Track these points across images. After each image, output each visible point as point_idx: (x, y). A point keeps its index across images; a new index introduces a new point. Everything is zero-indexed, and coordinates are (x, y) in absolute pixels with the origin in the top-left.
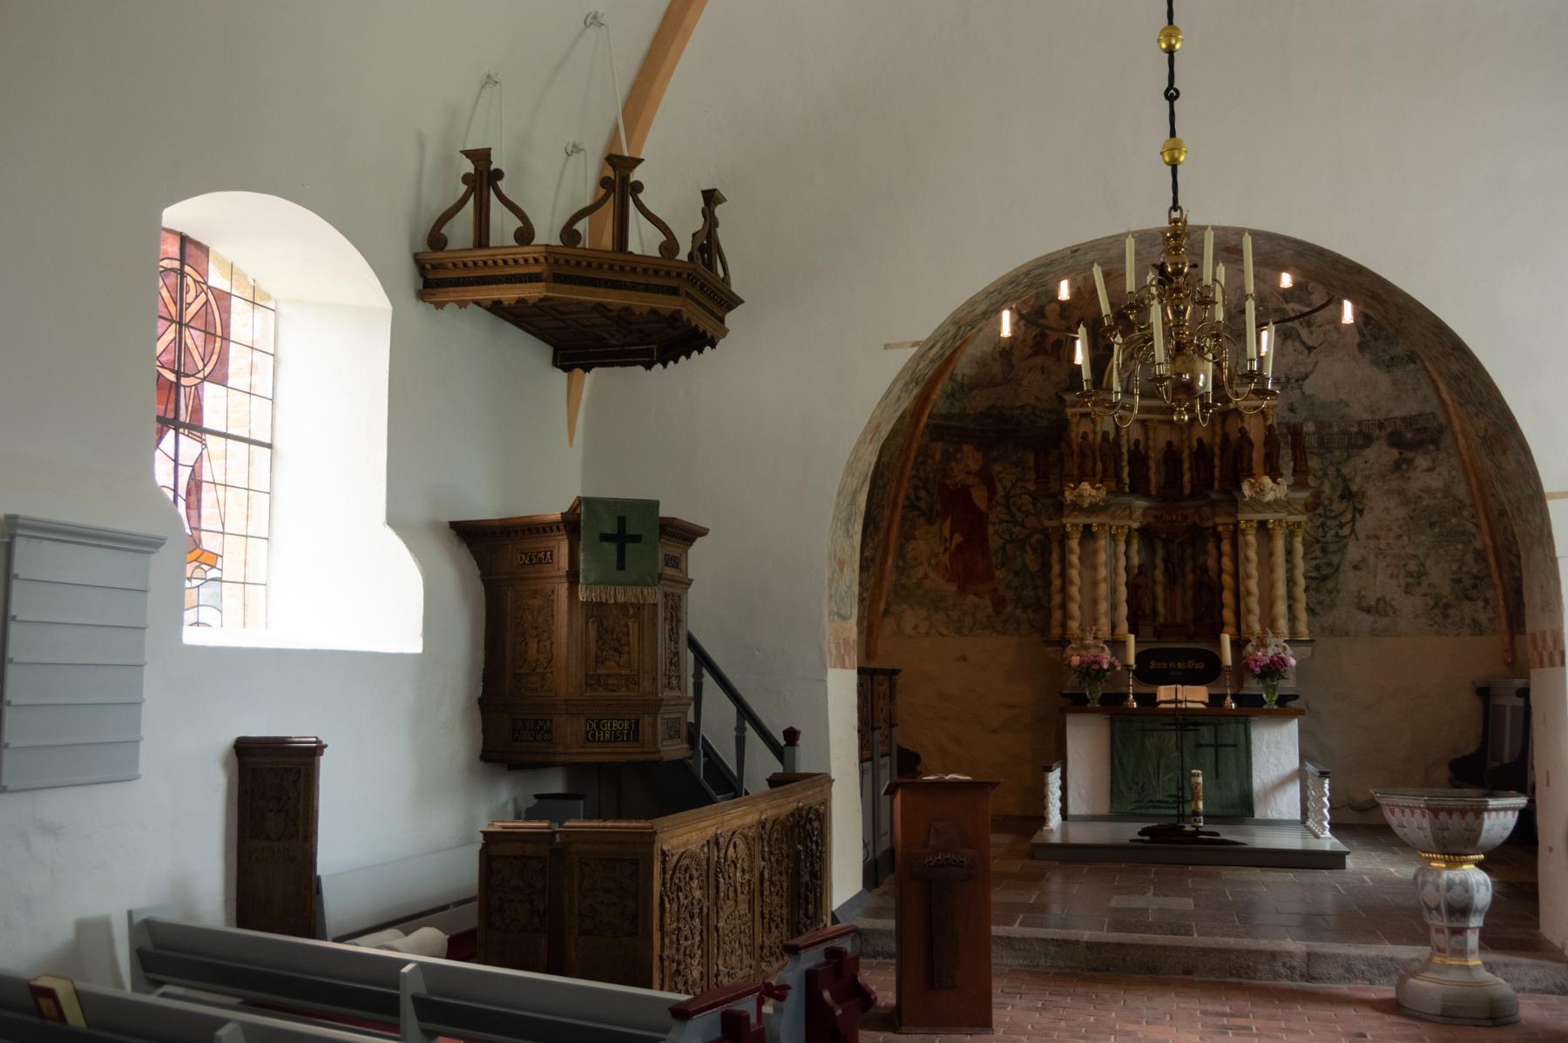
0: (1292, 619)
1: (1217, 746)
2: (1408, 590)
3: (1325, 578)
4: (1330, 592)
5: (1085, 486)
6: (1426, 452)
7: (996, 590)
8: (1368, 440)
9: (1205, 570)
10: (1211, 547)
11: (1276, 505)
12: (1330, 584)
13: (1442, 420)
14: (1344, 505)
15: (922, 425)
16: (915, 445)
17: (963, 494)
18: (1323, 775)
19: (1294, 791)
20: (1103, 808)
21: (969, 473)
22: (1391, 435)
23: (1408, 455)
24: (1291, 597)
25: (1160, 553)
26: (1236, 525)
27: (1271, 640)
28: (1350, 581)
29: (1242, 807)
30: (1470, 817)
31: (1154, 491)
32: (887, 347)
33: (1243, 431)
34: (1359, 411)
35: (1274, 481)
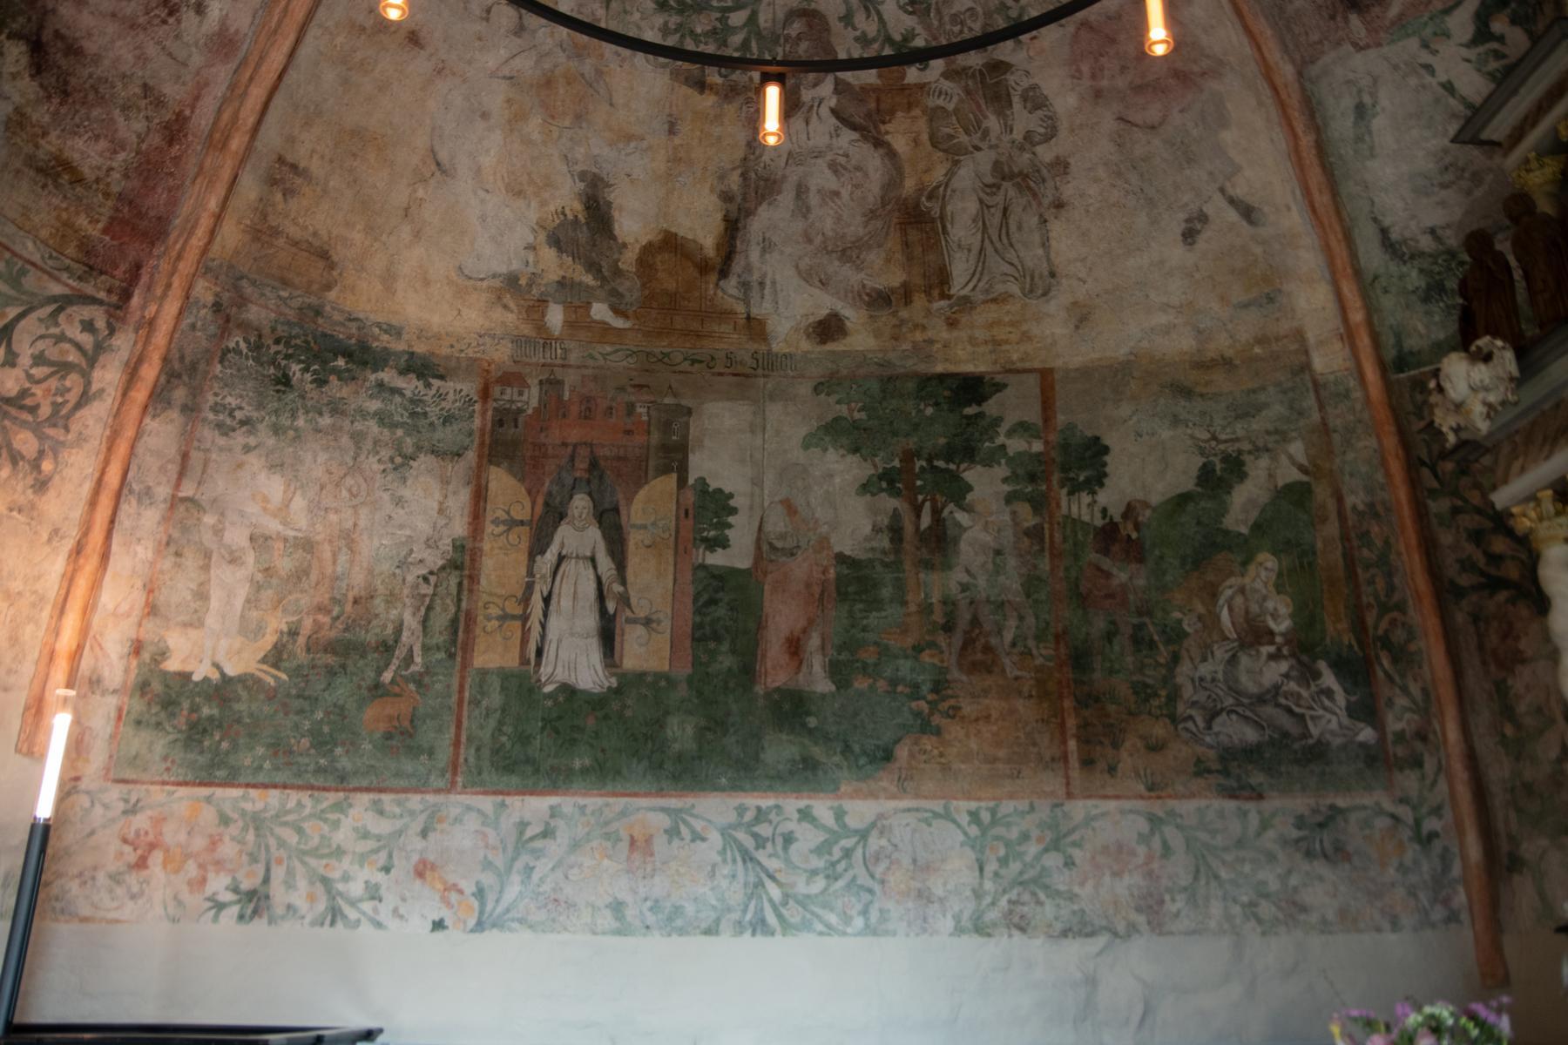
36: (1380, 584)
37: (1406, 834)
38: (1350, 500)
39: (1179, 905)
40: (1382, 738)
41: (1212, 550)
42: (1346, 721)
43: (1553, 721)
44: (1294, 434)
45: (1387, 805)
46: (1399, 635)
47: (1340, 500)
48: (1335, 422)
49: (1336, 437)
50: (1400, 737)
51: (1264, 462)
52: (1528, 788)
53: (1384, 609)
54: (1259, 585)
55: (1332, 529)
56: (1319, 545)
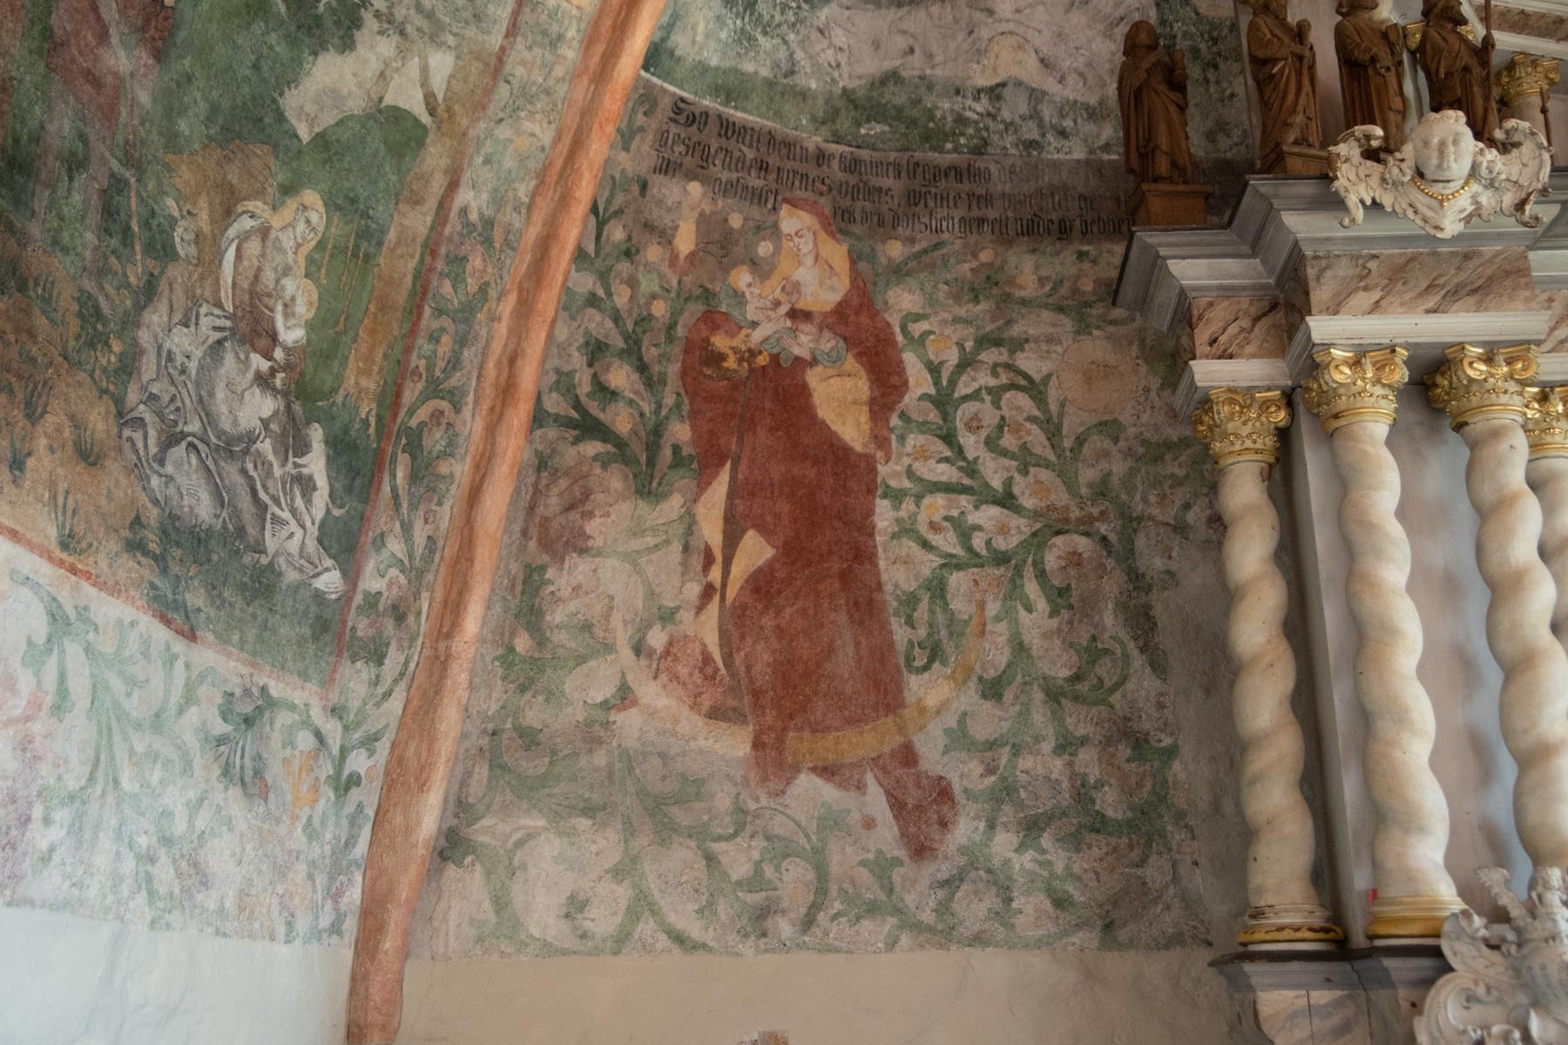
7: (908, 756)
16: (598, 148)
17: (779, 389)
36: (445, 347)
37: (327, 769)
38: (464, 196)
39: (56, 833)
40: (347, 597)
42: (312, 546)
43: (609, 648)
44: (451, 40)
45: (317, 716)
46: (435, 440)
47: (453, 186)
48: (516, 69)
49: (503, 89)
50: (372, 600)
51: (386, 47)
52: (529, 739)
53: (435, 389)
54: (288, 242)
55: (419, 221)
56: (392, 235)
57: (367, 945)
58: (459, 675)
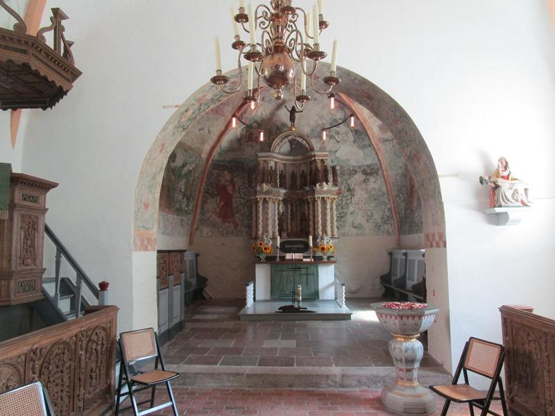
0: (332, 231)
1: (307, 275)
2: (368, 220)
3: (342, 217)
4: (344, 221)
5: (264, 185)
6: (374, 176)
8: (356, 172)
9: (304, 214)
10: (306, 207)
11: (328, 192)
12: (344, 219)
13: (379, 166)
14: (348, 193)
15: (209, 164)
16: (207, 171)
17: (224, 187)
18: (343, 285)
19: (332, 290)
20: (268, 298)
21: (226, 181)
22: (363, 171)
23: (368, 177)
24: (332, 223)
25: (290, 208)
26: (314, 198)
27: (325, 237)
28: (349, 218)
29: (314, 296)
30: (416, 319)
31: (287, 187)
32: (164, 107)
33: (316, 166)
34: (353, 163)
35: (327, 184)
41: (180, 177)
57: (190, 237)
58: (197, 216)
